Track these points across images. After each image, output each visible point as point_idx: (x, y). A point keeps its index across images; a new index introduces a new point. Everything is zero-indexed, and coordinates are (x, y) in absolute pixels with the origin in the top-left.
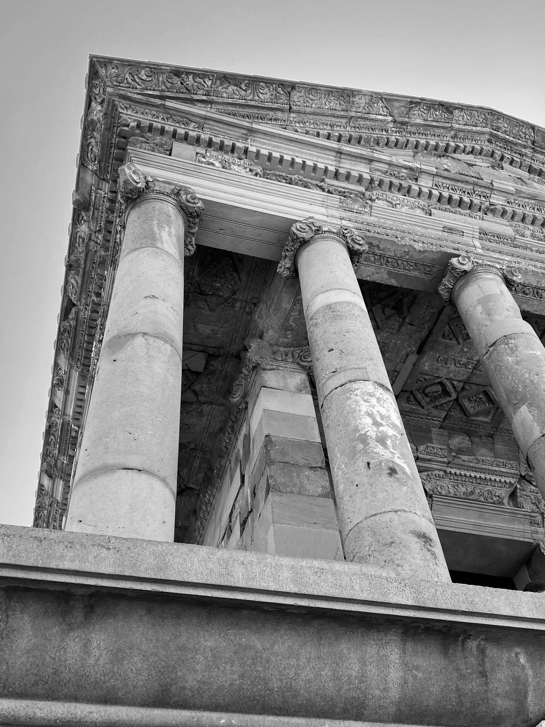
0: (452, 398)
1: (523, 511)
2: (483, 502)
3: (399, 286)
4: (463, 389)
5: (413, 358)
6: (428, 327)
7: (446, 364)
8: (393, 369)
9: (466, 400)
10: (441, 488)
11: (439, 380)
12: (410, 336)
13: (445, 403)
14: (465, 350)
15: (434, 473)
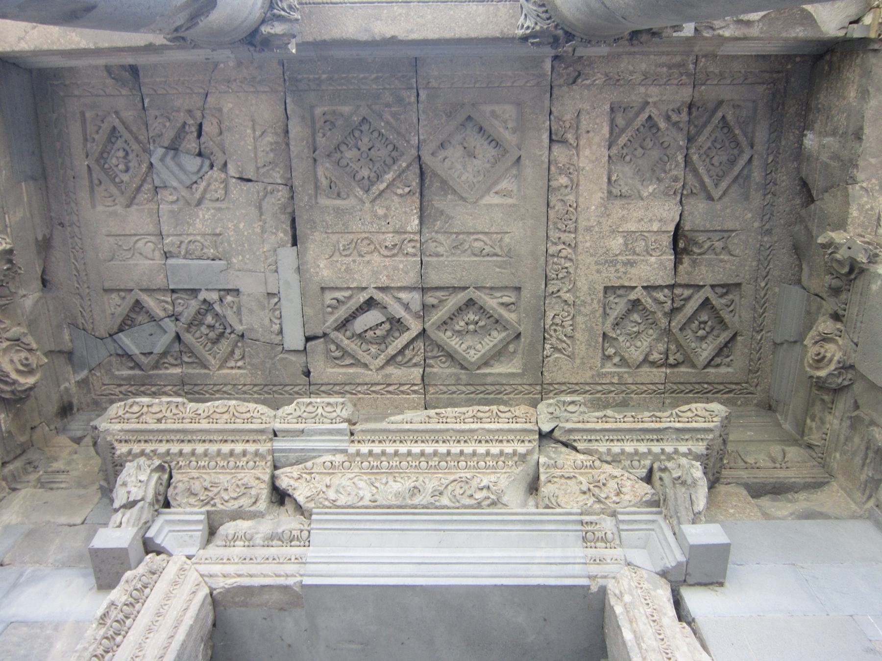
0: (415, 334)
1: (560, 514)
2: (448, 508)
3: (92, 46)
4: (424, 306)
5: (288, 255)
6: (282, 177)
7: (361, 256)
8: (263, 290)
9: (449, 333)
10: (337, 491)
11: (367, 297)
12: (260, 208)
13: (407, 346)
14: (381, 212)
15: (320, 460)
